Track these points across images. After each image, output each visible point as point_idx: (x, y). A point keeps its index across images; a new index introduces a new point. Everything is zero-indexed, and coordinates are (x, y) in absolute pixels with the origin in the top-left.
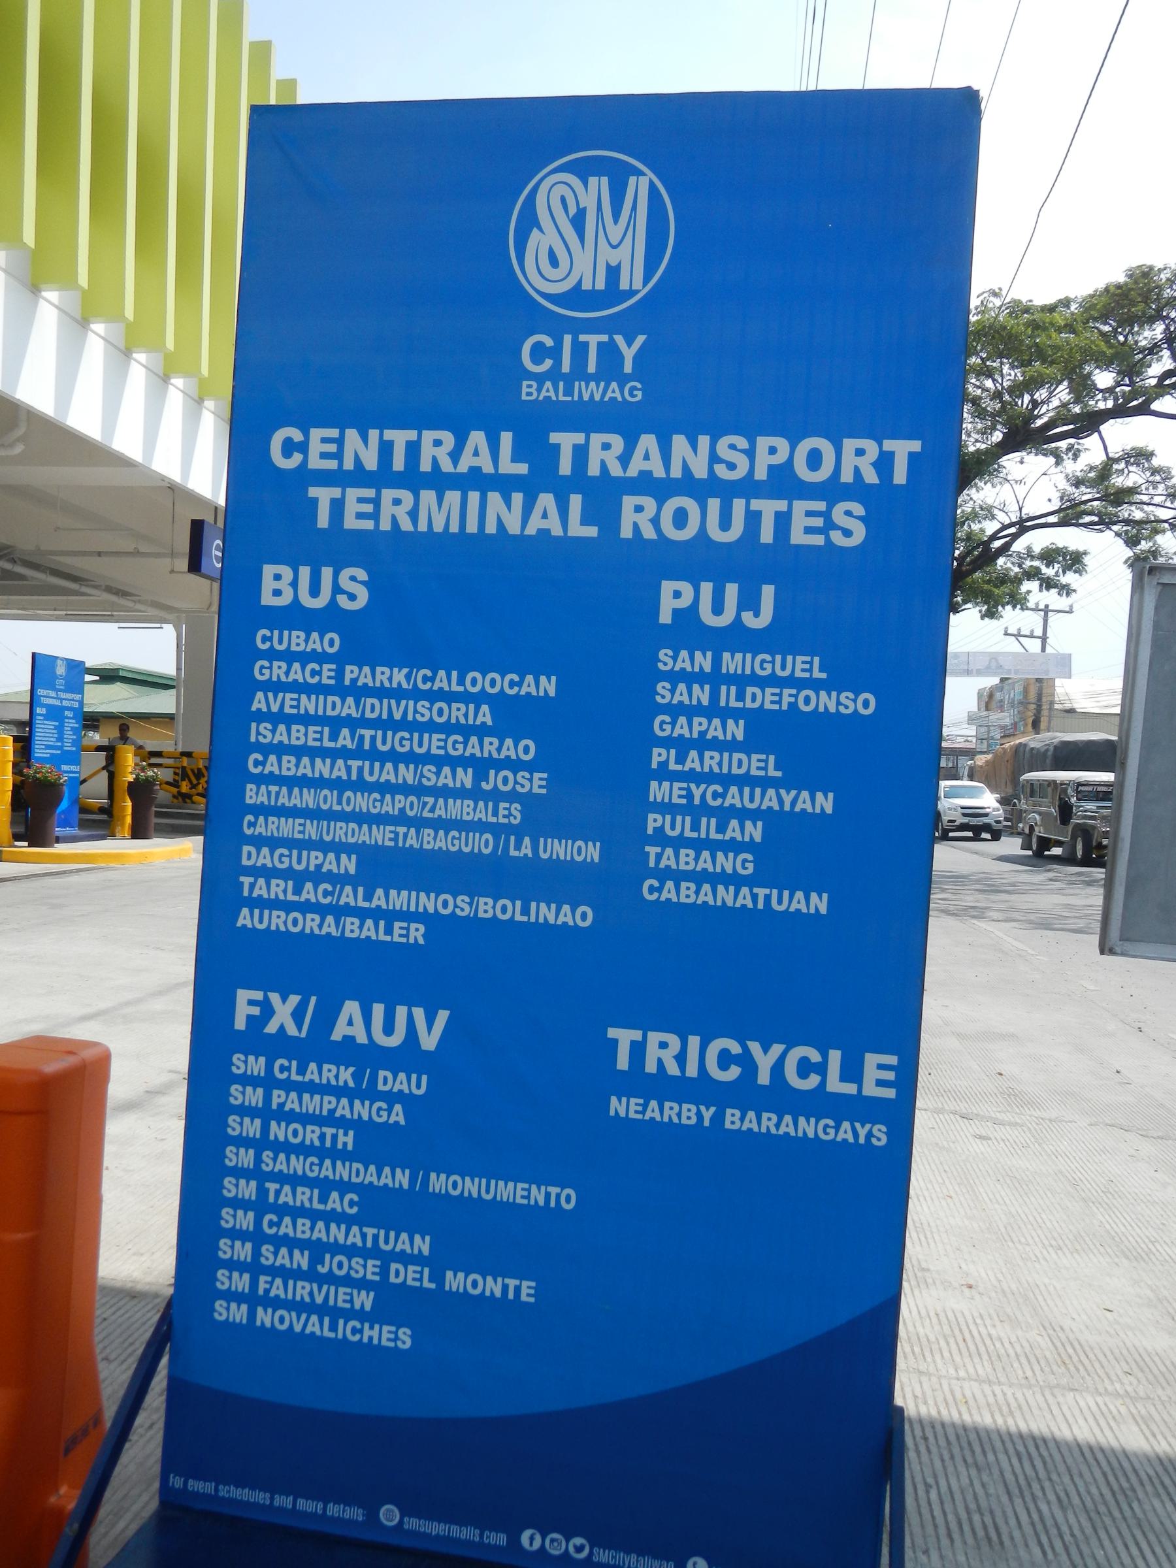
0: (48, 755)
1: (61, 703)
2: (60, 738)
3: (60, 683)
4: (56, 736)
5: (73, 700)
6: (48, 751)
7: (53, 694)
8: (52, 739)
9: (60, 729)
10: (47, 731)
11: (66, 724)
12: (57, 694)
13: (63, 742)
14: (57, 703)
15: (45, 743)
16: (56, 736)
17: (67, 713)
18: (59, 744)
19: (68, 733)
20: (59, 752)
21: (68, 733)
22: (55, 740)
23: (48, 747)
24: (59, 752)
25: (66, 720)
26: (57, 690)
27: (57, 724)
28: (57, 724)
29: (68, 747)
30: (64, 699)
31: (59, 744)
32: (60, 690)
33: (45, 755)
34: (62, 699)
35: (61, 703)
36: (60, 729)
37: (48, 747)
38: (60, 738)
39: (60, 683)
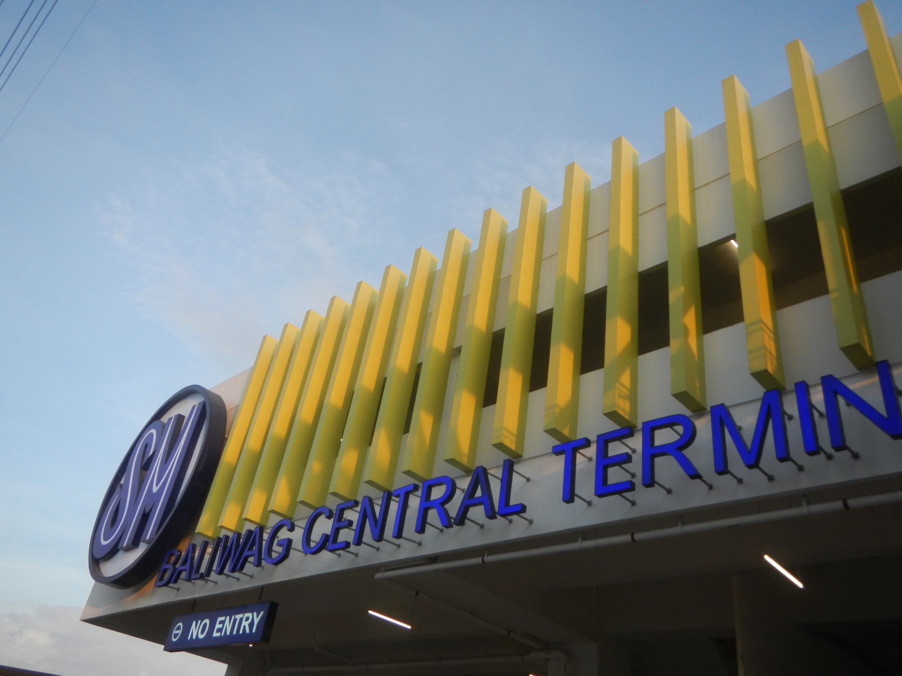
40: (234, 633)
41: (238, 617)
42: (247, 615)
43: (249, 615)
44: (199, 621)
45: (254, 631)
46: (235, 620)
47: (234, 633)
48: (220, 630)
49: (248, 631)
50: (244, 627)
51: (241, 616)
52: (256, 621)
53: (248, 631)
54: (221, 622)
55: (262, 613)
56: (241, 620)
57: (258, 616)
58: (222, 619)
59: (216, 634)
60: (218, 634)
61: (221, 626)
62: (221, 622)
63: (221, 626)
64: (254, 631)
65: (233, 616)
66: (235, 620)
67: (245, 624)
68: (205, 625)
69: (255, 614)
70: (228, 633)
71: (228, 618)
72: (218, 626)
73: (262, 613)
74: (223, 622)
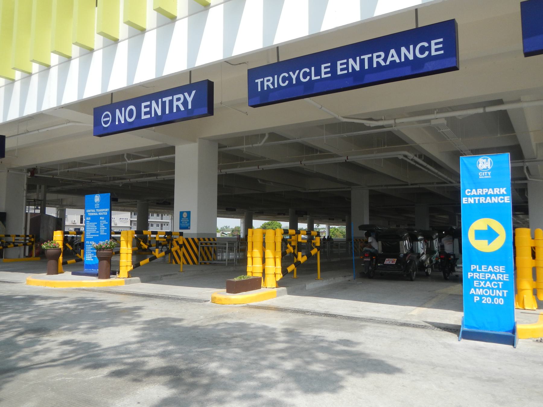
0: (92, 237)
1: (98, 214)
2: (98, 229)
3: (97, 206)
4: (96, 228)
5: (104, 212)
6: (92, 236)
7: (94, 211)
8: (94, 230)
9: (98, 226)
10: (92, 227)
11: (101, 223)
12: (96, 211)
13: (99, 231)
14: (96, 214)
15: (91, 232)
16: (96, 228)
17: (101, 218)
18: (98, 232)
19: (102, 227)
20: (98, 236)
21: (102, 227)
22: (95, 230)
23: (92, 234)
24: (98, 236)
25: (101, 221)
26: (95, 209)
27: (96, 223)
28: (96, 223)
29: (102, 233)
30: (100, 212)
31: (98, 232)
32: (97, 208)
33: (91, 237)
34: (98, 212)
35: (98, 214)
36: (98, 226)
37: (92, 234)
38: (98, 229)
39: (97, 206)
40: (167, 112)
41: (167, 99)
42: (175, 97)
43: (181, 96)
44: (123, 109)
45: (190, 107)
46: (164, 103)
47: (167, 112)
48: (146, 113)
49: (182, 109)
50: (178, 107)
51: (171, 98)
52: (190, 100)
53: (182, 109)
54: (146, 107)
55: (194, 92)
56: (171, 102)
57: (190, 96)
58: (148, 103)
59: (143, 117)
60: (148, 116)
61: (148, 109)
62: (146, 107)
63: (148, 109)
64: (190, 107)
65: (160, 100)
66: (164, 103)
67: (179, 103)
68: (131, 111)
69: (186, 94)
70: (159, 113)
71: (153, 102)
72: (143, 110)
73: (194, 92)
74: (150, 106)
